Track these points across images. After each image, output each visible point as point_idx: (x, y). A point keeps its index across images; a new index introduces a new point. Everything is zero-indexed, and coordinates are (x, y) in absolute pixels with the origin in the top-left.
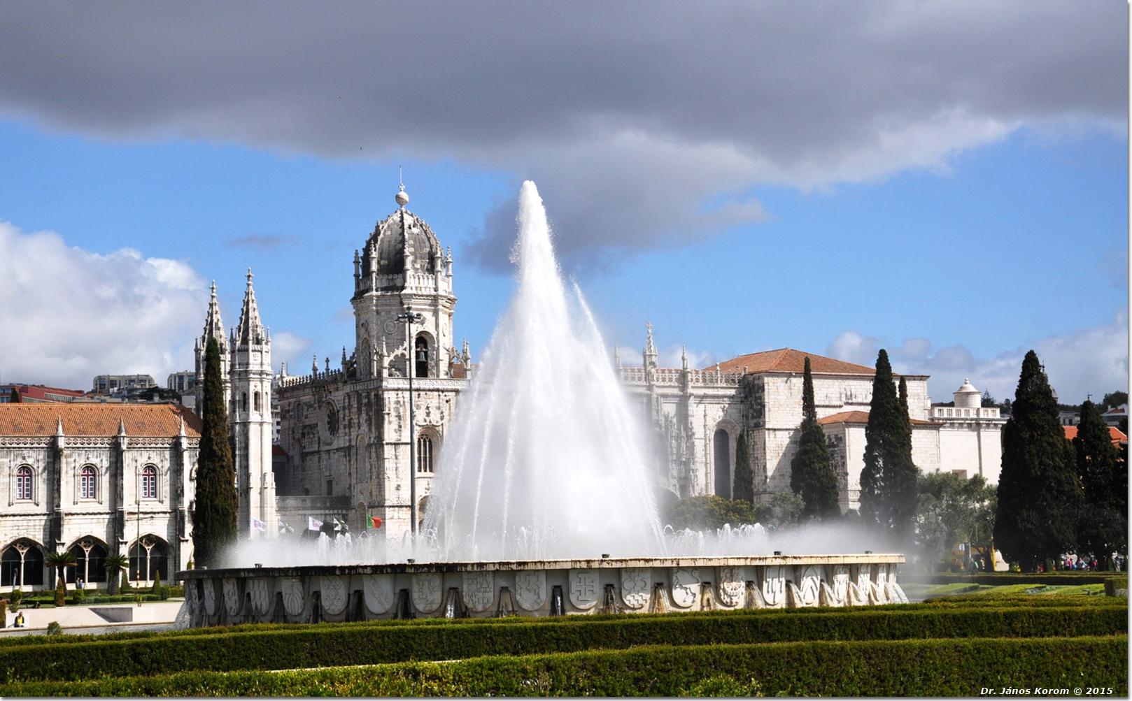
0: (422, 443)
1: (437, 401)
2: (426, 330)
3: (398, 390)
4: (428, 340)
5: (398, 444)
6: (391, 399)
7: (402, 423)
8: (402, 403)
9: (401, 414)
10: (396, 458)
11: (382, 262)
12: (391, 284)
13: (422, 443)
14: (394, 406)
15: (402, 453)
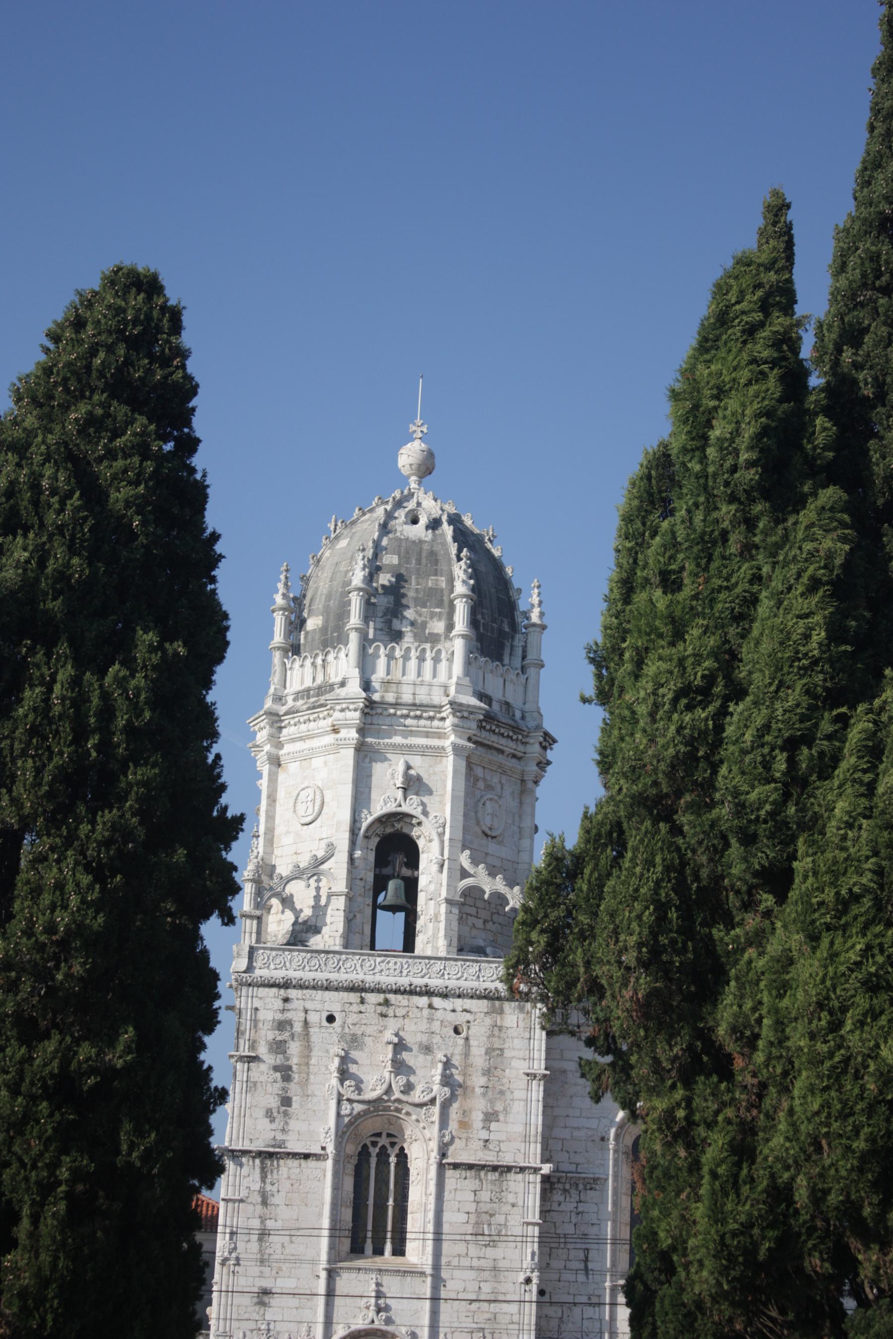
0: (373, 1161)
1: (423, 1026)
2: (405, 808)
3: (286, 985)
4: (421, 843)
5: (271, 1155)
6: (261, 1015)
7: (294, 1089)
8: (298, 1027)
9: (294, 1061)
10: (265, 1203)
11: (313, 623)
12: (320, 680)
13: (373, 1161)
14: (270, 1035)
15: (285, 1185)
